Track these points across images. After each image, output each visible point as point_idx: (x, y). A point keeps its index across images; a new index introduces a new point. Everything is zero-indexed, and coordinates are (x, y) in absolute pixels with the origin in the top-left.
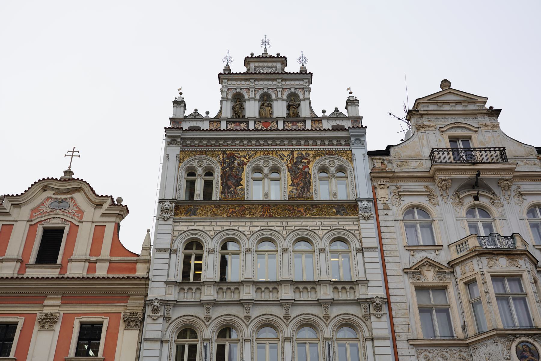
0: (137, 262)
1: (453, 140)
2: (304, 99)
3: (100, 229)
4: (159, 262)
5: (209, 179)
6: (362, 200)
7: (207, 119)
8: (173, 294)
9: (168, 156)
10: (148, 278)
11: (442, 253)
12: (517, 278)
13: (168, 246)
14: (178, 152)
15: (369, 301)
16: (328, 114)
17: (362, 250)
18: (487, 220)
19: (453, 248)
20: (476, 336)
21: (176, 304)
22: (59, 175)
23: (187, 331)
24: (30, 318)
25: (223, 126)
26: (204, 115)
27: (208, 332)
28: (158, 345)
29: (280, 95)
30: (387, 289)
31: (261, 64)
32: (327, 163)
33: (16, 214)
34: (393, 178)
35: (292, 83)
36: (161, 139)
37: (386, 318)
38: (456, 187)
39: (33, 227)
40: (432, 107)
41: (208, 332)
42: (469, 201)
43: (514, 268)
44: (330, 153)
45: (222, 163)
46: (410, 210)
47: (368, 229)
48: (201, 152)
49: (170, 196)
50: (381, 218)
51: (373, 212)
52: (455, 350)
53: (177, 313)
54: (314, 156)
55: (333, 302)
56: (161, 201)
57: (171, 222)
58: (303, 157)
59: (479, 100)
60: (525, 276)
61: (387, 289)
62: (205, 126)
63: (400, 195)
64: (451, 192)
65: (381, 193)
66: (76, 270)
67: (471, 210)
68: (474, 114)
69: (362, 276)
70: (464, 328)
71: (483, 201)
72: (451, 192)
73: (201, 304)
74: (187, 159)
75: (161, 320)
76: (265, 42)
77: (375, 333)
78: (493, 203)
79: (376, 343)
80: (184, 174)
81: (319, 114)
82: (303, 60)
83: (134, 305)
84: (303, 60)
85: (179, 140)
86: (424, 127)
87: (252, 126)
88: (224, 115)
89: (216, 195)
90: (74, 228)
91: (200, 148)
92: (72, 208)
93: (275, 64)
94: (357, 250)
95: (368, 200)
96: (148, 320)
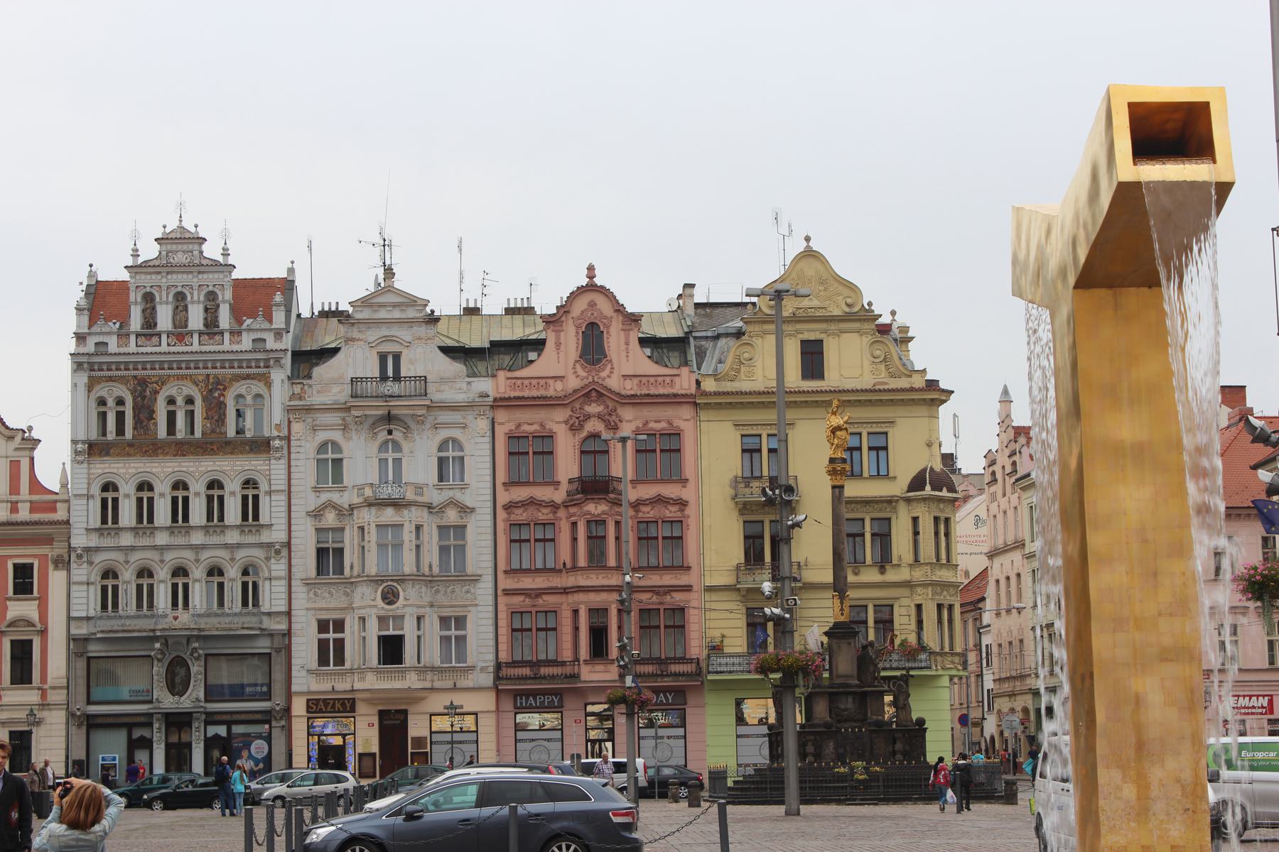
0: (56, 501)
1: (383, 358)
4: (78, 507)
5: (120, 408)
6: (274, 438)
8: (94, 541)
9: (75, 385)
11: (346, 494)
14: (86, 380)
15: (269, 545)
17: (270, 493)
21: (98, 549)
28: (85, 587)
29: (196, 298)
31: (174, 247)
34: (309, 410)
35: (211, 276)
36: (67, 365)
37: (284, 561)
38: (370, 421)
40: (365, 314)
42: (383, 435)
45: (133, 392)
46: (323, 447)
49: (82, 437)
50: (293, 456)
51: (285, 452)
52: (341, 587)
53: (99, 558)
56: (74, 442)
57: (85, 465)
58: (218, 383)
59: (419, 302)
60: (406, 524)
63: (314, 429)
64: (366, 425)
65: (296, 427)
68: (410, 322)
70: (352, 567)
74: (97, 388)
75: (85, 565)
77: (274, 574)
78: (406, 437)
79: (273, 583)
80: (93, 404)
85: (86, 366)
86: (353, 340)
89: (129, 434)
91: (110, 373)
93: (191, 247)
94: (266, 493)
96: (73, 565)
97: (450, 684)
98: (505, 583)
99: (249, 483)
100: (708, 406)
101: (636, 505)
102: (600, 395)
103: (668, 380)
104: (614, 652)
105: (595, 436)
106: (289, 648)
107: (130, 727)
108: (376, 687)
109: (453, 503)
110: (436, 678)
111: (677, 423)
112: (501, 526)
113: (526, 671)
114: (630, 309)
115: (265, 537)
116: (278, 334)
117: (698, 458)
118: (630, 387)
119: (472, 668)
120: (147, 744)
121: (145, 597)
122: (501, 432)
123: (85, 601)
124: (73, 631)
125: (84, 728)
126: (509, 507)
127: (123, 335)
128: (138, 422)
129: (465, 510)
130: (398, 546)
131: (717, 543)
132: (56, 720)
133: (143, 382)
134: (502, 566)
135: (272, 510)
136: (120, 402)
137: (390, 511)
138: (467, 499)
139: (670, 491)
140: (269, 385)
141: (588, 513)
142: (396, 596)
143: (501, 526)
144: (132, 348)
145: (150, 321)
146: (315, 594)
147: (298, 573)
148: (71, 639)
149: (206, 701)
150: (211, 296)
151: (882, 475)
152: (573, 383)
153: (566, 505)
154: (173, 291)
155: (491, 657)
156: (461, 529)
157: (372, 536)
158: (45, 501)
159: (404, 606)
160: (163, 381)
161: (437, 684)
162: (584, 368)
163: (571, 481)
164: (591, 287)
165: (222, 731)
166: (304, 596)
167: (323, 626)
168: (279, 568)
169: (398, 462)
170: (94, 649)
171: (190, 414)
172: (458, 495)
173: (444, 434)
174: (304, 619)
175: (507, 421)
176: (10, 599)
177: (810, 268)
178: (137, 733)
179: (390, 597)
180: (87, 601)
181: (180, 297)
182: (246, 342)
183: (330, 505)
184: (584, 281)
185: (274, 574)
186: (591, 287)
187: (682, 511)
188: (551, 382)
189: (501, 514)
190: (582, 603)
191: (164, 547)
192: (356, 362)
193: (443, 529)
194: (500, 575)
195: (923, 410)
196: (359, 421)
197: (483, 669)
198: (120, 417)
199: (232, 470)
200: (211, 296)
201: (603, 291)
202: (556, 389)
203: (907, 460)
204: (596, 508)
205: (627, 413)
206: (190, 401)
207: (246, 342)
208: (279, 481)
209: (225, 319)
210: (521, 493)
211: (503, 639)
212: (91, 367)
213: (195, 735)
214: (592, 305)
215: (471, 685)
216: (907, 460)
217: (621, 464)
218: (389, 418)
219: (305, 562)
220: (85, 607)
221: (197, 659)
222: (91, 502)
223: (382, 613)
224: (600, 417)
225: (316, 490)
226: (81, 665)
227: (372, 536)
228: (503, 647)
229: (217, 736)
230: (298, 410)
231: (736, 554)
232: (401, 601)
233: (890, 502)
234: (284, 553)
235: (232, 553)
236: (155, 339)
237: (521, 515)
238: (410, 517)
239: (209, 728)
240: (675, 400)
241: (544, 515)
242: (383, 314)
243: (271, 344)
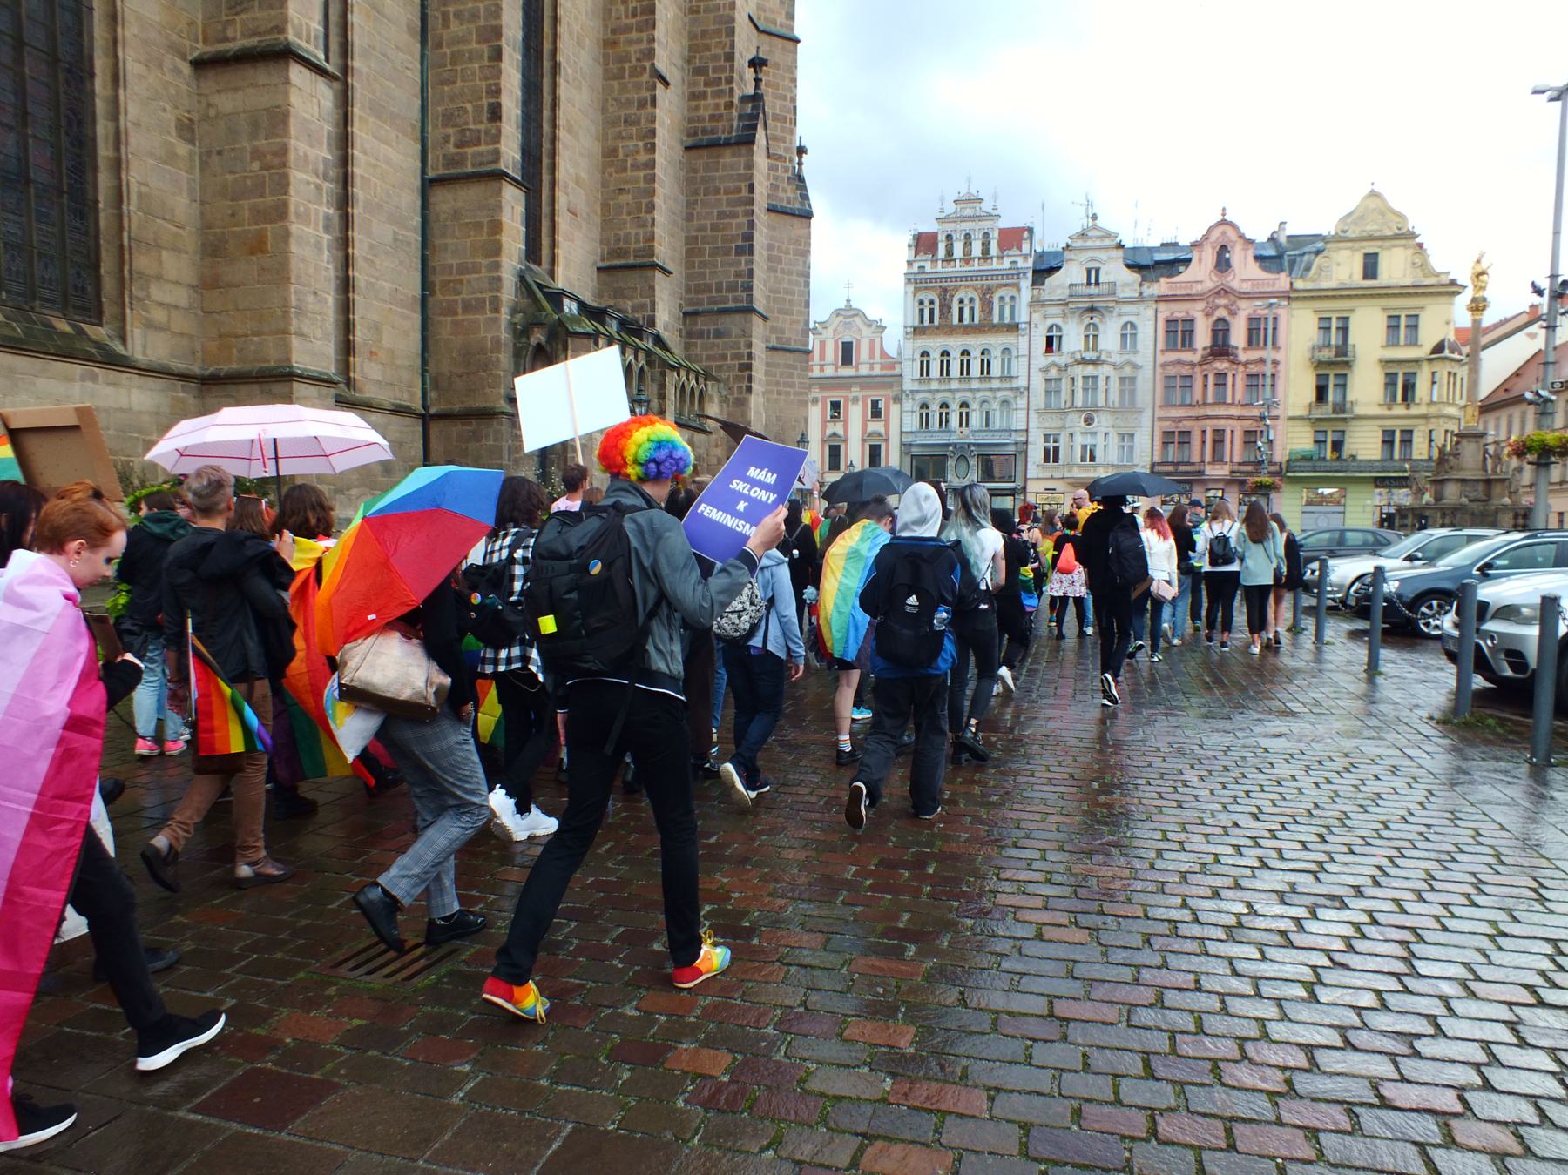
1: (1089, 271)
3: (872, 342)
8: (916, 386)
36: (902, 280)
39: (836, 343)
40: (1079, 244)
42: (1087, 321)
53: (918, 396)
65: (1035, 316)
66: (864, 370)
67: (1087, 328)
68: (1106, 248)
71: (1096, 320)
82: (995, 197)
84: (995, 197)
89: (936, 322)
98: (1160, 413)
99: (1006, 350)
100: (1297, 299)
101: (1246, 364)
104: (1227, 459)
109: (1129, 363)
113: (1170, 468)
114: (1248, 236)
116: (1025, 257)
117: (1288, 333)
118: (1246, 287)
121: (944, 421)
122: (1161, 318)
126: (1164, 365)
127: (934, 261)
129: (1136, 367)
130: (1095, 389)
133: (945, 290)
134: (1158, 403)
135: (1019, 367)
136: (932, 302)
137: (1090, 367)
138: (1138, 360)
140: (1019, 290)
143: (1158, 377)
144: (939, 269)
145: (950, 253)
148: (902, 444)
150: (986, 235)
151: (1413, 342)
152: (1209, 285)
153: (1200, 364)
156: (1133, 379)
157: (1079, 383)
158: (890, 363)
160: (956, 289)
164: (1224, 222)
167: (1047, 437)
168: (1022, 403)
169: (1095, 336)
171: (972, 309)
172: (1133, 358)
173: (1125, 319)
175: (1165, 311)
177: (1373, 203)
179: (1089, 421)
180: (912, 422)
181: (968, 236)
182: (1006, 263)
183: (1054, 364)
184: (1220, 218)
186: (1224, 222)
189: (1159, 370)
191: (956, 391)
192: (1071, 275)
193: (1122, 379)
196: (1073, 312)
198: (932, 312)
199: (996, 342)
200: (986, 235)
201: (1231, 224)
202: (1198, 288)
203: (1430, 335)
204: (1222, 365)
205: (1243, 304)
206: (971, 300)
207: (1006, 263)
208: (1024, 349)
209: (994, 249)
210: (1172, 356)
212: (916, 281)
214: (1224, 233)
216: (1430, 335)
217: (1238, 337)
218: (1092, 309)
219: (1038, 400)
224: (1226, 307)
227: (1079, 383)
228: (1156, 453)
230: (1036, 303)
231: (1311, 395)
233: (1417, 361)
237: (1172, 371)
241: (1186, 371)
242: (1089, 243)
243: (1021, 264)
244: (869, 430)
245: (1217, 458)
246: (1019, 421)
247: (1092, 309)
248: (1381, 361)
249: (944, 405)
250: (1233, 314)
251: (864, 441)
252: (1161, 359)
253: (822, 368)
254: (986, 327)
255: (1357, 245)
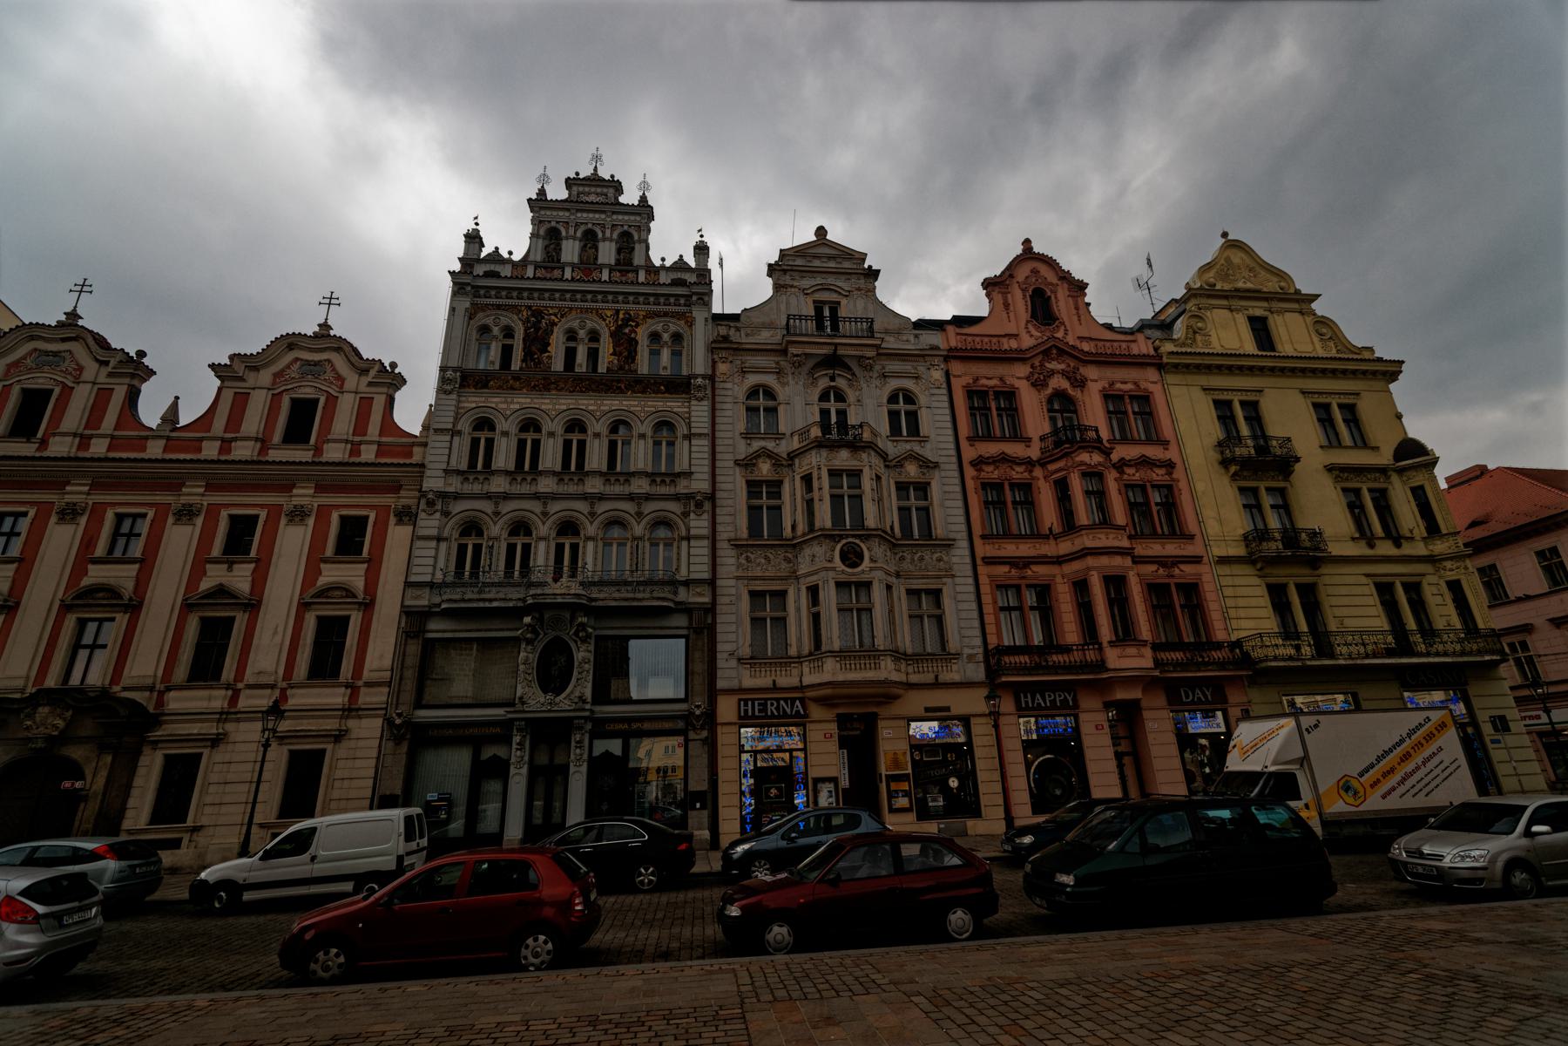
0: (413, 444)
2: (640, 241)
6: (696, 376)
7: (509, 261)
8: (455, 485)
9: (452, 310)
10: (423, 465)
12: (855, 474)
13: (450, 426)
14: (468, 305)
15: (689, 497)
16: (668, 263)
17: (689, 437)
18: (841, 406)
19: (796, 438)
20: (804, 535)
21: (457, 496)
22: (310, 329)
23: (472, 527)
24: (275, 511)
25: (530, 272)
26: (506, 256)
27: (496, 529)
28: (433, 544)
29: (608, 234)
30: (714, 482)
32: (659, 328)
33: (251, 379)
34: (738, 349)
36: (447, 285)
38: (811, 363)
39: (276, 399)
40: (799, 262)
41: (496, 529)
43: (855, 463)
44: (666, 314)
46: (753, 393)
47: (700, 413)
48: (499, 307)
49: (454, 363)
51: (709, 392)
52: (781, 552)
53: (457, 507)
54: (645, 317)
55: (648, 497)
56: (443, 369)
57: (454, 396)
58: (630, 319)
60: (866, 471)
61: (714, 482)
62: (506, 271)
63: (744, 372)
64: (805, 369)
65: (722, 368)
66: (334, 453)
67: (824, 397)
68: (847, 274)
69: (685, 467)
70: (794, 527)
71: (841, 383)
72: (805, 369)
73: (488, 496)
74: (481, 315)
75: (438, 515)
76: (597, 158)
77: (693, 532)
78: (851, 386)
79: (693, 543)
81: (657, 263)
82: (645, 185)
83: (407, 498)
84: (645, 185)
87: (568, 274)
88: (531, 258)
89: (516, 365)
90: (332, 401)
92: (329, 375)
95: (704, 377)
96: (422, 515)
97: (929, 678)
98: (982, 549)
99: (664, 425)
102: (1061, 352)
103: (1124, 345)
105: (1060, 395)
106: (712, 630)
107: (477, 744)
108: (841, 678)
110: (910, 669)
111: (1143, 385)
112: (970, 484)
114: (1077, 275)
115: (682, 487)
119: (957, 656)
120: (500, 769)
121: (518, 559)
123: (431, 561)
124: (407, 603)
125: (404, 748)
126: (978, 463)
128: (528, 355)
129: (928, 465)
131: (1217, 512)
132: (368, 730)
133: (538, 314)
136: (508, 332)
137: (844, 454)
138: (928, 452)
139: (1153, 452)
140: (691, 323)
141: (1082, 463)
142: (861, 557)
146: (747, 558)
147: (724, 533)
148: (407, 612)
149: (594, 703)
153: (1042, 463)
154: (583, 228)
155: (978, 642)
156: (923, 489)
159: (872, 569)
161: (914, 678)
162: (1037, 328)
163: (1042, 439)
165: (615, 746)
166: (732, 561)
170: (437, 628)
171: (593, 355)
173: (894, 384)
174: (733, 591)
175: (964, 375)
176: (326, 561)
178: (488, 752)
179: (852, 557)
180: (434, 562)
185: (693, 532)
187: (1170, 474)
188: (1005, 340)
189: (970, 472)
190: (1094, 568)
193: (902, 487)
194: (977, 542)
195: (1378, 385)
197: (971, 657)
205: (1091, 372)
206: (594, 336)
210: (991, 449)
211: (989, 619)
213: (575, 752)
214: (1035, 272)
215: (957, 678)
219: (734, 520)
220: (430, 570)
221: (584, 641)
222: (456, 439)
223: (843, 578)
224: (1063, 373)
225: (748, 436)
226: (414, 648)
229: (607, 754)
232: (866, 563)
234: (707, 506)
235: (639, 505)
236: (557, 273)
237: (992, 473)
238: (868, 464)
239: (597, 743)
240: (1140, 362)
241: (1018, 473)
244: (322, 581)
245: (1126, 634)
246: (695, 562)
247: (833, 362)
248: (1330, 469)
249: (520, 527)
250: (1081, 383)
251: (304, 606)
252: (969, 453)
253: (226, 445)
254: (624, 381)
255: (1236, 303)
